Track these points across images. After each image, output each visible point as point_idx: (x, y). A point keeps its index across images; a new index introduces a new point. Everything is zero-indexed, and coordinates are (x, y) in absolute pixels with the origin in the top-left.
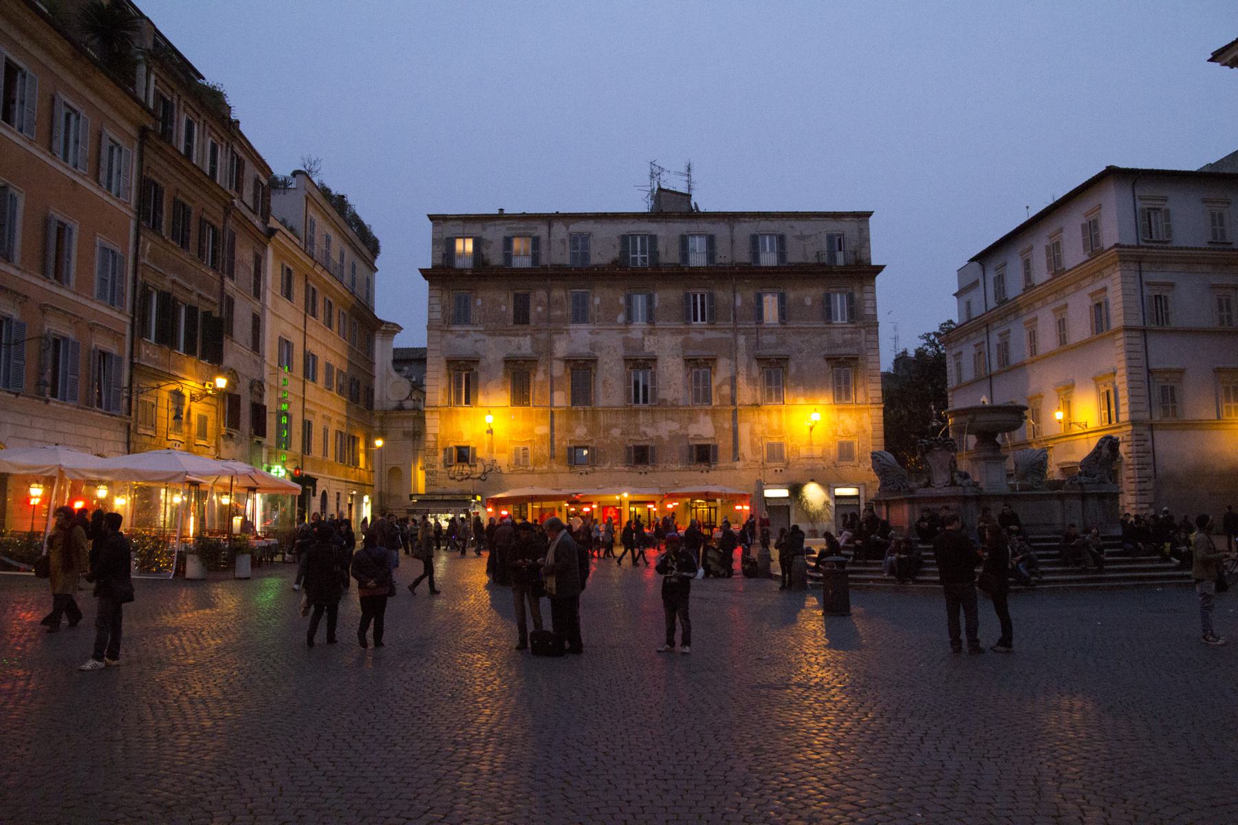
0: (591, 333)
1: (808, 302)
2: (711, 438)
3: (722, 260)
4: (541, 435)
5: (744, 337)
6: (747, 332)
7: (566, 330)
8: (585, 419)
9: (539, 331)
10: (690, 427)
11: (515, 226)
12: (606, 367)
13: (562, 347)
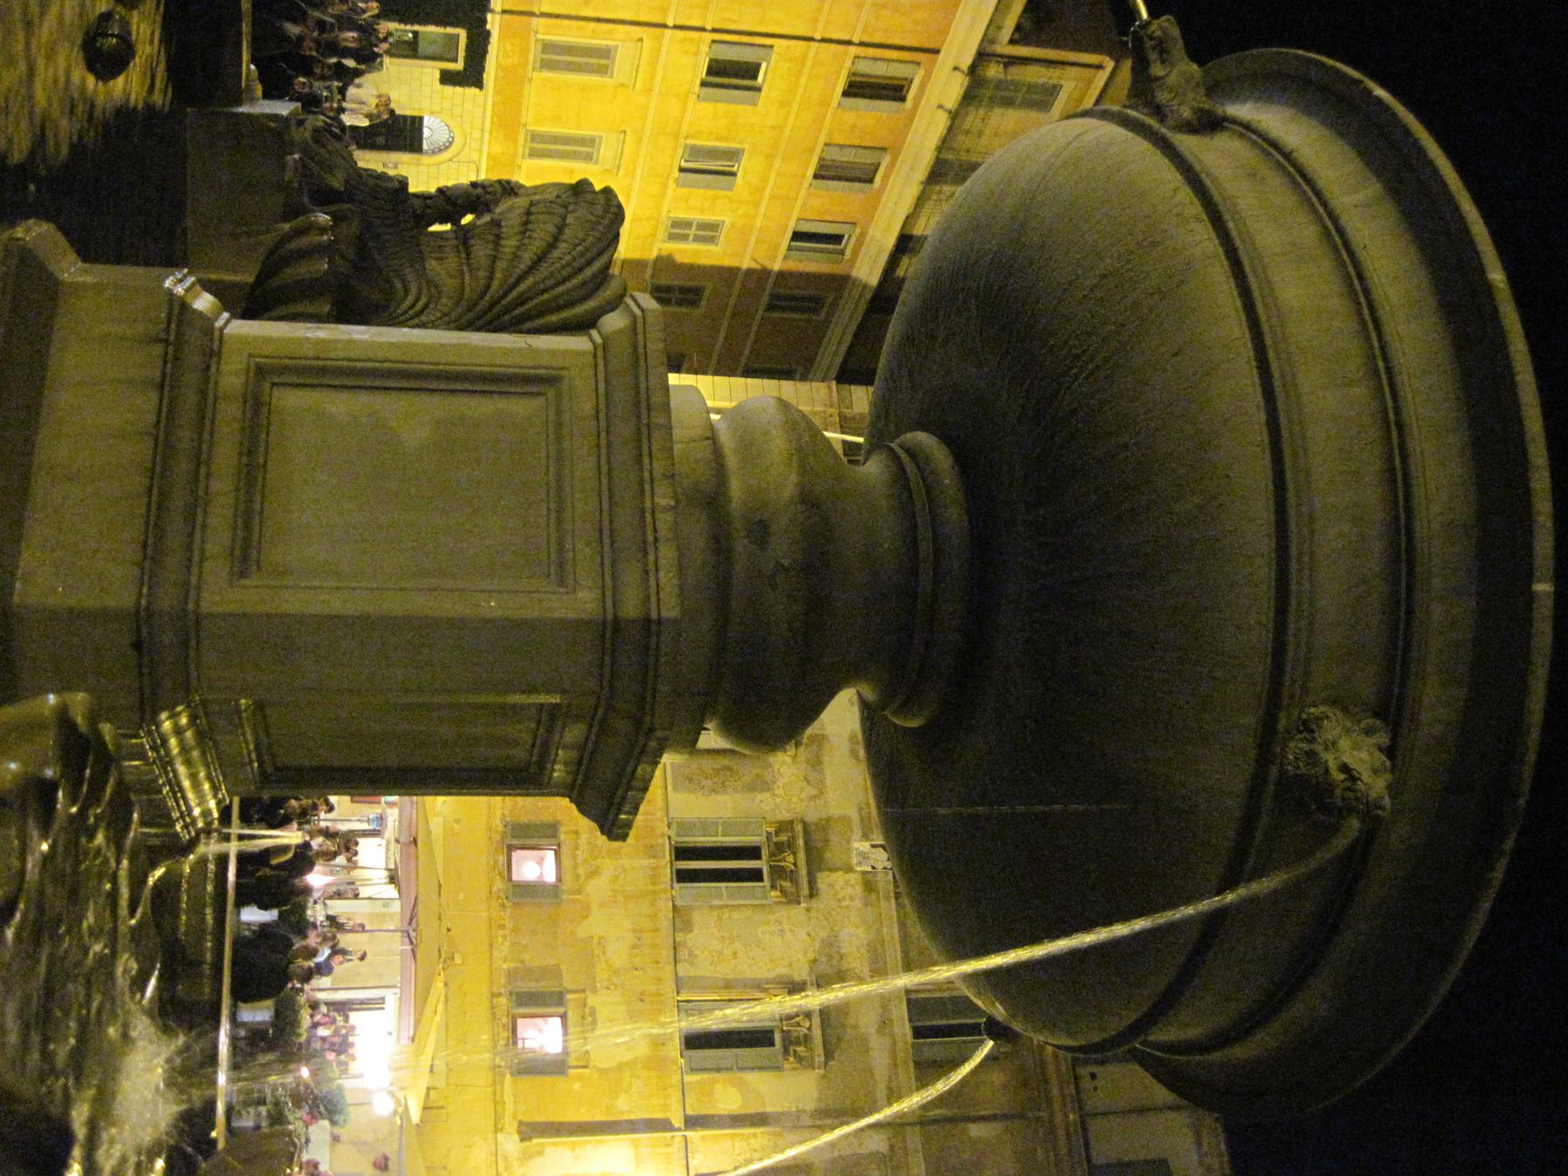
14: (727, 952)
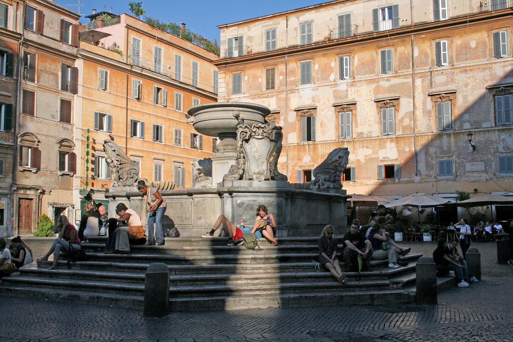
0: (313, 90)
1: (473, 44)
2: (396, 160)
3: (405, 24)
4: (282, 163)
5: (420, 79)
6: (423, 76)
7: (297, 90)
8: (309, 151)
9: (280, 92)
10: (380, 152)
11: (266, 24)
12: (323, 113)
13: (295, 102)
14: (368, 123)
